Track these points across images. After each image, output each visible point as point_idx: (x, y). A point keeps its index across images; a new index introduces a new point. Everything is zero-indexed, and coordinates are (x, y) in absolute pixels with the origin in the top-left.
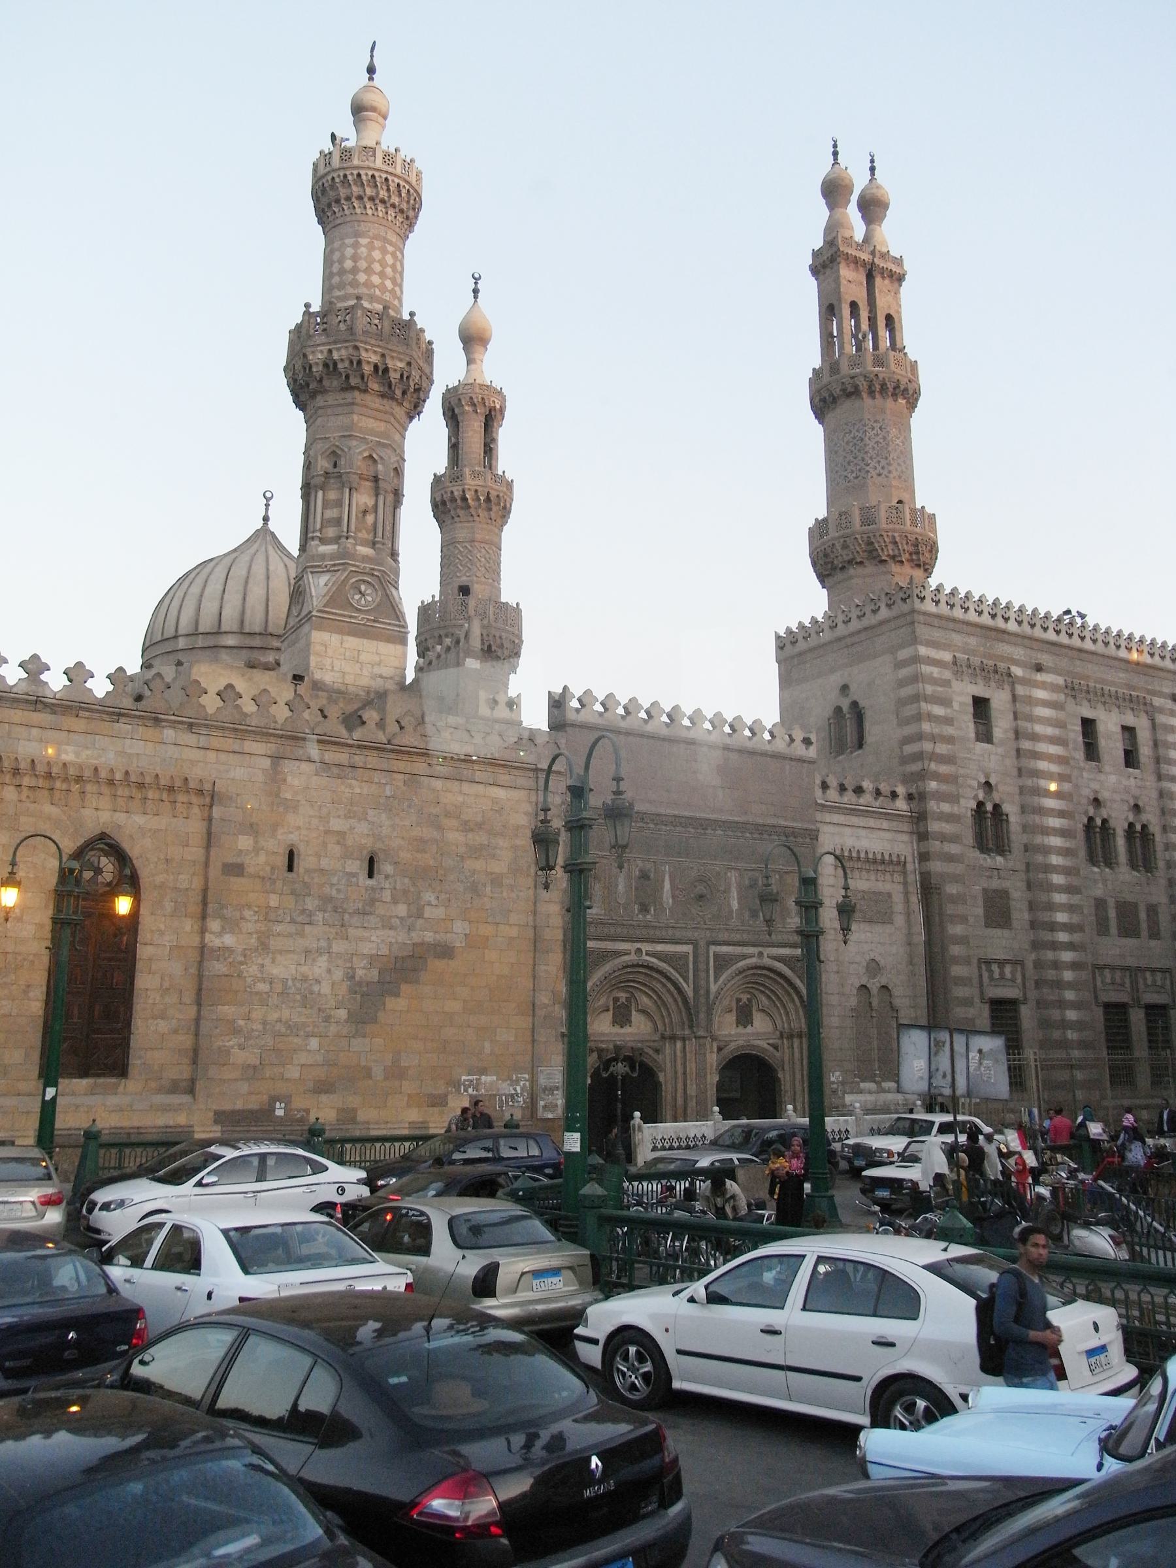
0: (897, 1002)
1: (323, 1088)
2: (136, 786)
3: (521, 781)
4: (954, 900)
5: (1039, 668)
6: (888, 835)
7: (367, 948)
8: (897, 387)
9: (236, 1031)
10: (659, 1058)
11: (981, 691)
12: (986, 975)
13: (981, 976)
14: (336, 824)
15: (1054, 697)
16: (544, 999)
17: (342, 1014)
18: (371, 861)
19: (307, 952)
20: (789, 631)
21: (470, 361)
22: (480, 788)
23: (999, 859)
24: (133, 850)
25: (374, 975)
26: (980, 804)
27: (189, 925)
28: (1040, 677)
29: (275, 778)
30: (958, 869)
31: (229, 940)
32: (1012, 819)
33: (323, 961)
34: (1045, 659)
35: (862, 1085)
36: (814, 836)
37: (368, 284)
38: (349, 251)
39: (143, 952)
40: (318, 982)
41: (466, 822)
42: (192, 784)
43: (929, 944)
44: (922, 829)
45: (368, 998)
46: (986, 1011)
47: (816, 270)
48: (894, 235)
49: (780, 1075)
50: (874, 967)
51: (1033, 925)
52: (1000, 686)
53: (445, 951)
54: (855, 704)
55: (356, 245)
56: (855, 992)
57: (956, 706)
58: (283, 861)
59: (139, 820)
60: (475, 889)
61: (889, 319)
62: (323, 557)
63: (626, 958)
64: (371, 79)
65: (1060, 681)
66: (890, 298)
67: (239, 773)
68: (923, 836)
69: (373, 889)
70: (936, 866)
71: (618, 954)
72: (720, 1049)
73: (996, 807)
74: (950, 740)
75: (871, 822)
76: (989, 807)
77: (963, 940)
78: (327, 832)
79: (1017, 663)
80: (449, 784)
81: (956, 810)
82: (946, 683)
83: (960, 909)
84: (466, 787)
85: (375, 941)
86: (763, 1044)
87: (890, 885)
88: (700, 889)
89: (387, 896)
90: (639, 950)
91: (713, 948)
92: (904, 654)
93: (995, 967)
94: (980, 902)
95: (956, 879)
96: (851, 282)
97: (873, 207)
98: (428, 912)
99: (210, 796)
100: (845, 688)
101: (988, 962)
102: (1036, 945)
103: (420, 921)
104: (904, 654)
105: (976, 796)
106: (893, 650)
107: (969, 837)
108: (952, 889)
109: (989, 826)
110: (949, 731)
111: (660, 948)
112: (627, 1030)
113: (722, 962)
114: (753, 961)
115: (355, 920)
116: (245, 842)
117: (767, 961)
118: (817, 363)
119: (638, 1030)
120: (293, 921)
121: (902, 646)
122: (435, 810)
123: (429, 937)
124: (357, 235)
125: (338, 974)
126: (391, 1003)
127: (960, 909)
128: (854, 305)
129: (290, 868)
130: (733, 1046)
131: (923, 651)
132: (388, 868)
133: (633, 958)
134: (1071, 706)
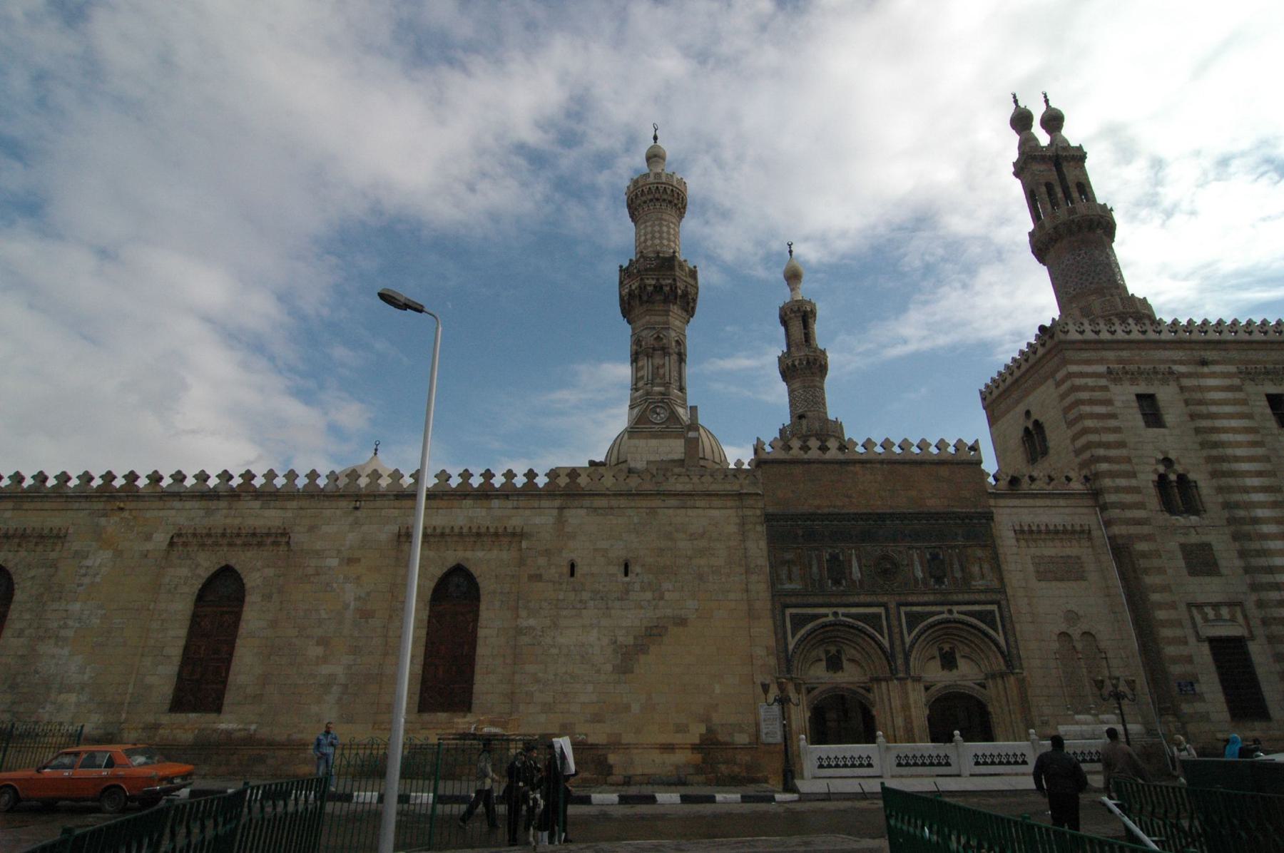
0: (1102, 645)
1: (597, 719)
2: (478, 536)
3: (730, 504)
4: (1144, 555)
5: (1204, 363)
6: (1067, 510)
9: (537, 681)
10: (871, 696)
11: (1143, 388)
12: (1198, 618)
13: (1192, 618)
15: (1227, 382)
16: (759, 652)
17: (609, 667)
18: (626, 566)
19: (584, 626)
20: (987, 386)
21: (792, 290)
22: (700, 511)
23: (1193, 518)
24: (475, 571)
25: (631, 641)
28: (1206, 370)
29: (560, 521)
30: (1146, 530)
31: (532, 622)
32: (1200, 484)
33: (595, 633)
34: (1210, 355)
35: (1078, 717)
36: (989, 517)
39: (481, 633)
40: (592, 646)
41: (691, 535)
42: (509, 530)
43: (1130, 597)
44: (1101, 502)
45: (627, 658)
46: (1206, 648)
48: (1072, 133)
49: (990, 709)
50: (1072, 617)
51: (1247, 570)
52: (1164, 381)
53: (682, 622)
54: (1036, 423)
56: (1055, 637)
57: (1118, 404)
58: (566, 570)
60: (701, 577)
63: (824, 620)
65: (1232, 369)
66: (1077, 172)
67: (537, 520)
68: (1104, 508)
69: (628, 583)
70: (1116, 530)
72: (927, 689)
74: (1117, 430)
75: (1048, 502)
76: (1173, 477)
77: (1166, 588)
78: (596, 550)
79: (1175, 362)
80: (679, 511)
81: (1134, 482)
82: (1105, 388)
83: (1156, 562)
84: (690, 512)
85: (630, 619)
86: (970, 684)
87: (1072, 549)
89: (637, 587)
90: (835, 614)
91: (903, 609)
92: (1059, 376)
93: (1208, 610)
94: (1179, 555)
95: (1148, 538)
96: (1046, 172)
97: (1053, 121)
98: (667, 596)
99: (517, 536)
100: (1028, 413)
101: (1200, 606)
102: (1255, 587)
103: (661, 603)
104: (1059, 376)
105: (1155, 471)
106: (1053, 374)
107: (1153, 501)
109: (1176, 492)
110: (1112, 423)
111: (854, 610)
112: (840, 674)
113: (913, 620)
114: (945, 616)
115: (617, 604)
116: (542, 561)
117: (956, 615)
118: (1030, 226)
119: (849, 676)
120: (574, 608)
121: (1057, 370)
123: (669, 612)
125: (605, 641)
126: (642, 658)
127: (1156, 562)
129: (572, 574)
130: (940, 685)
131: (1074, 368)
133: (831, 618)
134: (1250, 388)
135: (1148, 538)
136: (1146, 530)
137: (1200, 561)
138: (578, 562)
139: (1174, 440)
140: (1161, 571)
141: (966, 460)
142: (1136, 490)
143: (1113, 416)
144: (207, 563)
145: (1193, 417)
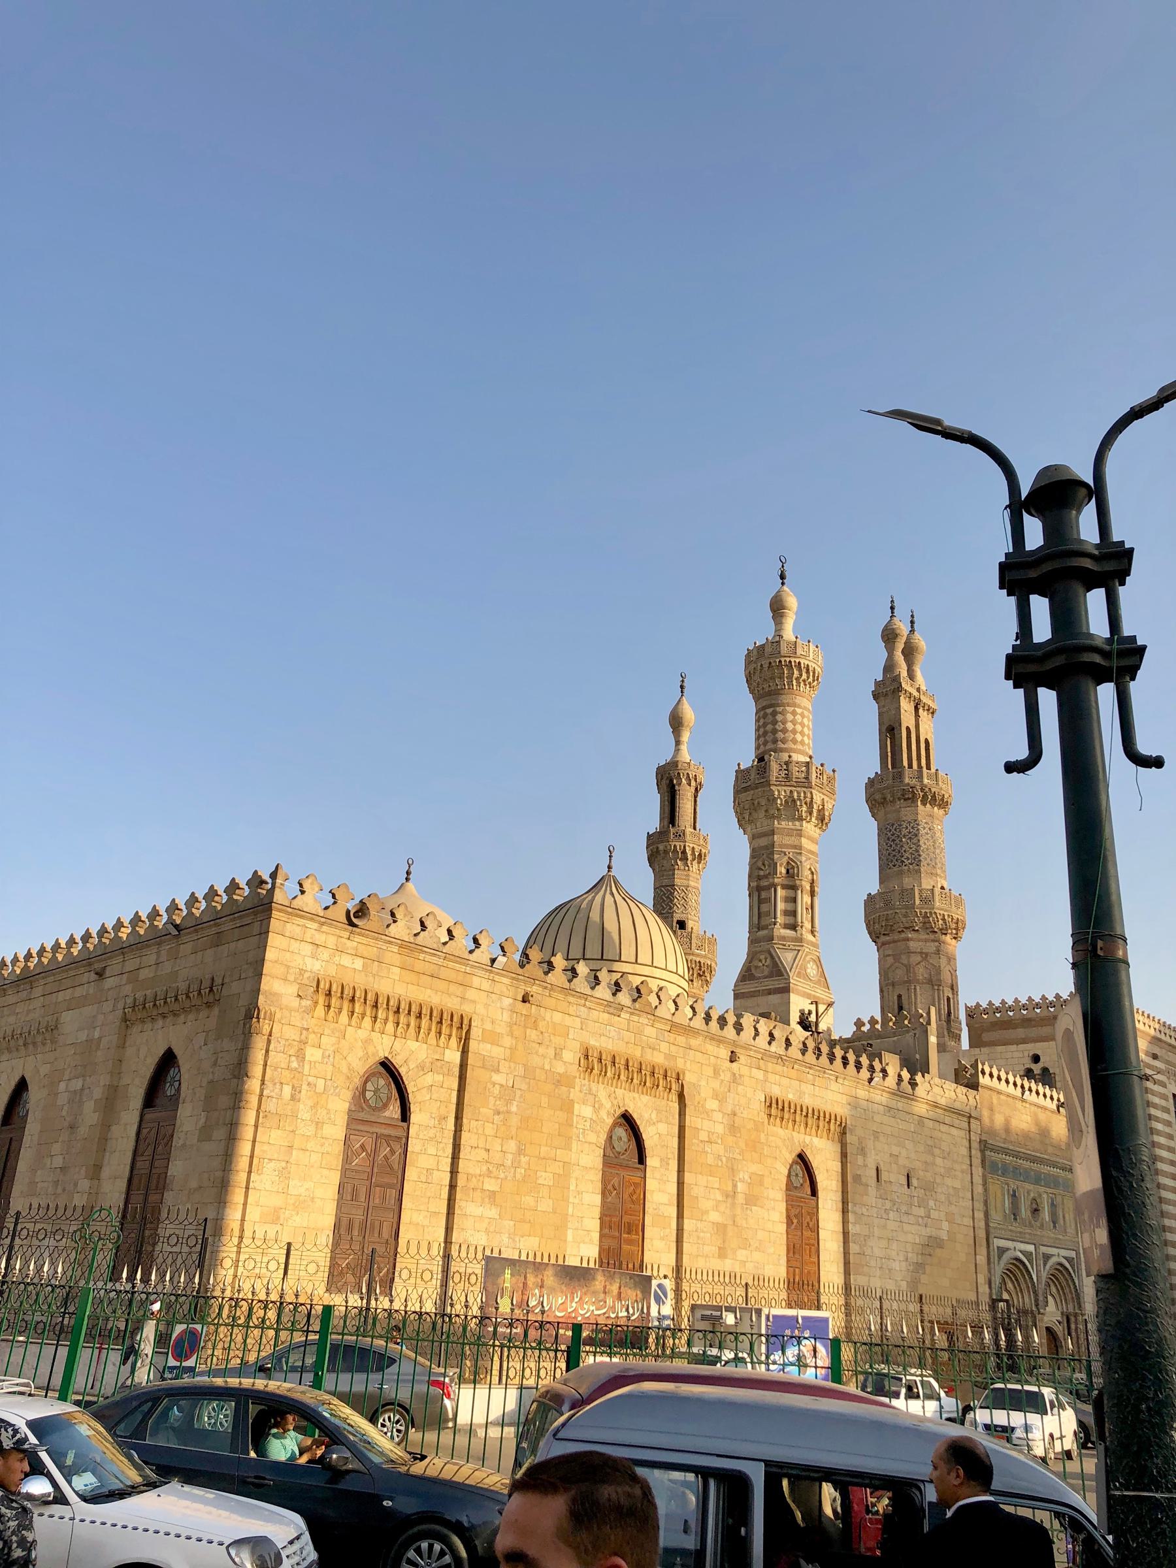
7: (910, 1238)
8: (942, 799)
14: (895, 1150)
27: (838, 1216)
38: (790, 717)
47: (876, 696)
55: (794, 713)
59: (816, 1141)
61: (927, 742)
62: (783, 938)
64: (783, 584)
71: (1008, 1249)
88: (1035, 1206)
100: (1036, 1059)
122: (930, 1142)
124: (795, 705)
128: (908, 729)
132: (914, 1182)
138: (882, 1167)
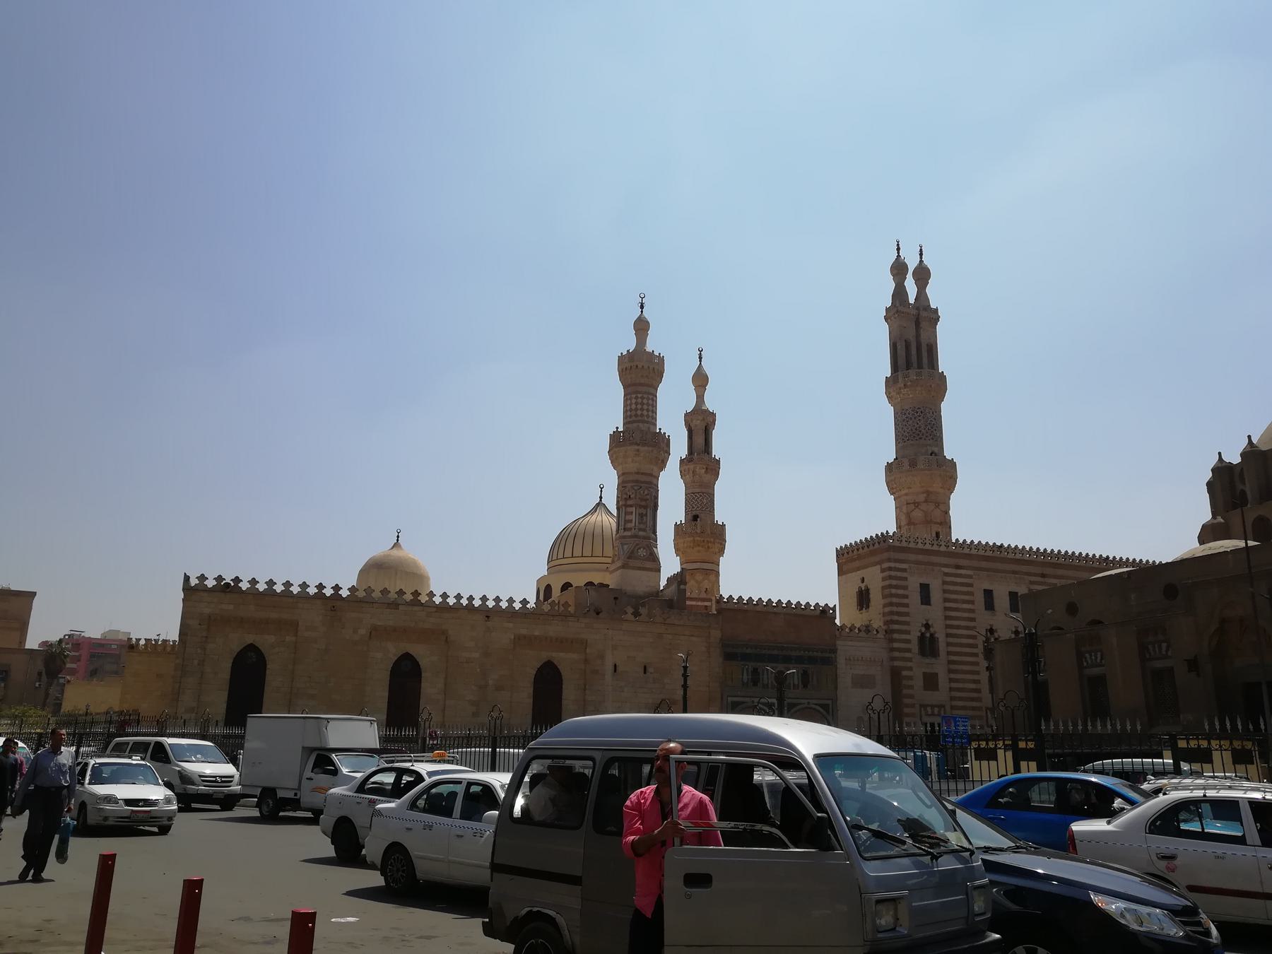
26: (922, 634)
36: (834, 651)
37: (642, 415)
48: (936, 295)
70: (896, 663)
73: (932, 635)
83: (910, 683)
95: (910, 669)
100: (863, 580)
108: (904, 673)
109: (928, 645)
127: (910, 683)
135: (910, 669)
136: (909, 664)
137: (931, 682)
139: (935, 613)
140: (911, 687)
141: (825, 613)
142: (908, 641)
143: (907, 597)
144: (393, 650)
145: (946, 600)
